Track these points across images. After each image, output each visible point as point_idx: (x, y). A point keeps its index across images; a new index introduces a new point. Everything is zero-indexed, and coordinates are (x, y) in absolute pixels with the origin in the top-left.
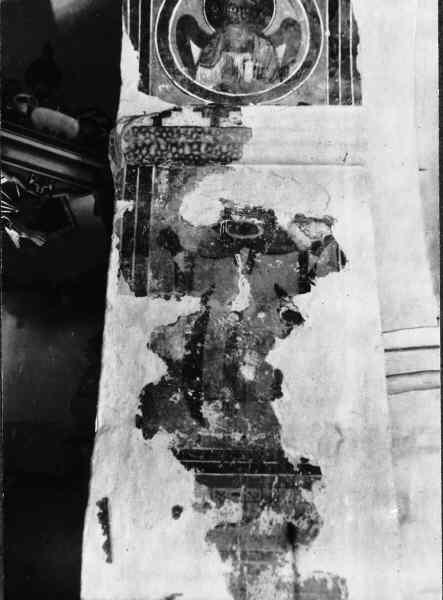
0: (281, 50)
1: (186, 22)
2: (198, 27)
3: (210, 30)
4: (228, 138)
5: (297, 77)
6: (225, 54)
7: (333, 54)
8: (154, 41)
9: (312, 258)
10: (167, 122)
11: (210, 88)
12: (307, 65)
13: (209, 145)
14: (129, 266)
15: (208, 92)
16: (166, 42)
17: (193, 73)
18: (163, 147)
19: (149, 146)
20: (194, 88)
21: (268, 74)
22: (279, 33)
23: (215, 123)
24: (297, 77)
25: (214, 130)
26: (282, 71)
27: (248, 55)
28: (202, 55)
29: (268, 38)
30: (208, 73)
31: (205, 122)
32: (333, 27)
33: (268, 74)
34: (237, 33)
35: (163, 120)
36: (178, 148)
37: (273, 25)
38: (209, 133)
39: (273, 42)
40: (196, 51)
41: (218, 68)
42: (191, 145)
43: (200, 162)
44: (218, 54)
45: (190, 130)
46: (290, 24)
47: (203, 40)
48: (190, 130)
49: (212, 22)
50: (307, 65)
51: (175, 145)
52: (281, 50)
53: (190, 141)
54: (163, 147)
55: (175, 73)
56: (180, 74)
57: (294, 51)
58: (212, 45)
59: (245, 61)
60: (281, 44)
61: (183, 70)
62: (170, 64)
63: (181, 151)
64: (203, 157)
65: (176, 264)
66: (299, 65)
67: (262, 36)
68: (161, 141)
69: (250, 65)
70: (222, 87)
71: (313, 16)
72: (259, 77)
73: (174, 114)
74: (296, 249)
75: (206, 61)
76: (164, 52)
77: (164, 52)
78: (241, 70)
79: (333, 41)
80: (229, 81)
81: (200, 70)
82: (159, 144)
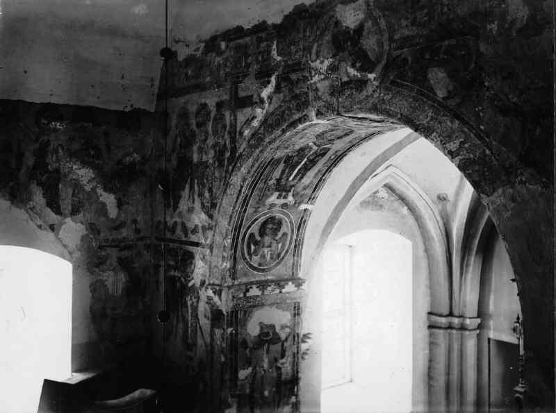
0: (280, 245)
1: (252, 235)
5: (283, 258)
8: (239, 245)
9: (285, 344)
10: (248, 294)
12: (287, 252)
17: (251, 259)
20: (251, 266)
21: (274, 256)
22: (280, 238)
26: (279, 255)
27: (269, 249)
33: (274, 256)
34: (267, 239)
37: (280, 235)
39: (278, 243)
40: (253, 247)
41: (259, 256)
43: (254, 306)
46: (285, 234)
47: (256, 243)
50: (287, 252)
55: (245, 259)
61: (247, 257)
62: (243, 254)
66: (285, 251)
69: (269, 253)
70: (260, 265)
71: (292, 231)
72: (272, 258)
75: (256, 253)
76: (242, 248)
77: (242, 248)
79: (296, 240)
80: (262, 261)
81: (254, 257)
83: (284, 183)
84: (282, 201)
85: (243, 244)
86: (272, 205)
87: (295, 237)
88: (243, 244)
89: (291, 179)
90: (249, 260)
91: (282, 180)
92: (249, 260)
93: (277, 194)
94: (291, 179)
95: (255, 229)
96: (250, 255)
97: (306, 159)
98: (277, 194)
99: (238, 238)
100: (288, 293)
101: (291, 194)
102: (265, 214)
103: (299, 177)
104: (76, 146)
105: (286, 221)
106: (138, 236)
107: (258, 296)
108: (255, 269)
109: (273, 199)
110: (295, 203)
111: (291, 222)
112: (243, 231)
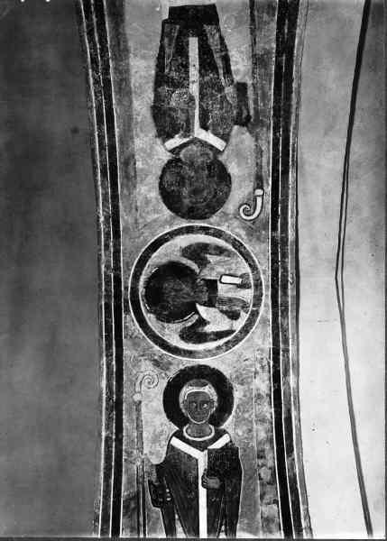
97: (203, 492)
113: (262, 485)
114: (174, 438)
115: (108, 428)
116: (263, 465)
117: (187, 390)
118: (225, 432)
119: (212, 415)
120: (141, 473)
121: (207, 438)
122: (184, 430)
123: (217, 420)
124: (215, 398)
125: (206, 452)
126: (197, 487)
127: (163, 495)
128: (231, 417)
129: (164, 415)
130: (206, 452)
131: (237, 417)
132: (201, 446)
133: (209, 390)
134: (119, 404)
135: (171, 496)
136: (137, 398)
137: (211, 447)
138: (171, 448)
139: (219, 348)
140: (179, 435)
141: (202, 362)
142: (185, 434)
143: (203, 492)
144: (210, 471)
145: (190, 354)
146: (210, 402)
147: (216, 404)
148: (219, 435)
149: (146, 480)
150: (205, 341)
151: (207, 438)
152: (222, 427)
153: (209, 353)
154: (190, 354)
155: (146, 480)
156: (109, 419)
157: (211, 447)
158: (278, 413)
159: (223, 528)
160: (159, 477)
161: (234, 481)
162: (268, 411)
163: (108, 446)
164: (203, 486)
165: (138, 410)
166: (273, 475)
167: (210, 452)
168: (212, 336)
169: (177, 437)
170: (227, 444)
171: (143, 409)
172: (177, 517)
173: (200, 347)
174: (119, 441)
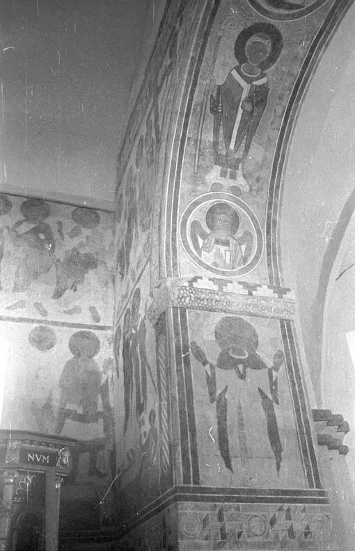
0: (243, 247)
1: (195, 224)
2: (202, 230)
3: (208, 231)
4: (227, 298)
5: (252, 264)
6: (215, 245)
7: (269, 254)
9: (275, 374)
10: (195, 285)
11: (209, 264)
13: (217, 301)
14: (181, 370)
15: (208, 266)
16: (185, 233)
17: (200, 255)
18: (193, 299)
19: (185, 298)
20: (201, 263)
23: (220, 289)
24: (252, 264)
25: (220, 293)
26: (245, 260)
27: (227, 248)
28: (204, 243)
29: (236, 240)
30: (208, 255)
31: (215, 288)
32: (268, 239)
35: (194, 284)
36: (201, 300)
37: (240, 234)
38: (217, 294)
40: (200, 241)
42: (207, 300)
44: (212, 245)
45: (208, 291)
47: (204, 236)
48: (208, 291)
49: (209, 226)
50: (257, 258)
51: (199, 299)
52: (243, 247)
53: (207, 297)
54: (193, 299)
55: (190, 252)
56: (193, 253)
57: (249, 249)
58: (209, 239)
59: (225, 251)
60: (243, 244)
61: (194, 251)
62: (187, 247)
63: (202, 302)
64: (214, 307)
65: (206, 371)
67: (234, 238)
68: (192, 295)
69: (228, 253)
71: (259, 231)
73: (199, 280)
74: (266, 367)
76: (185, 241)
77: (185, 241)
78: (224, 256)
80: (218, 261)
81: (203, 253)
82: (190, 297)
83: (224, 153)
84: (231, 183)
85: (183, 233)
86: (217, 187)
87: (265, 242)
88: (183, 233)
89: (232, 146)
90: (197, 255)
91: (220, 147)
92: (197, 255)
93: (217, 169)
94: (232, 146)
95: (198, 215)
96: (196, 247)
97: (240, 111)
98: (217, 169)
99: (175, 222)
100: (265, 299)
101: (239, 172)
102: (209, 198)
103: (243, 145)
104: (25, 228)
105: (245, 216)
106: (97, 324)
107: (212, 292)
108: (208, 268)
109: (214, 175)
110: (251, 189)
111: (253, 218)
112: (180, 215)
113: (275, 116)
114: (234, 70)
115: (195, 49)
116: (280, 104)
117: (255, 39)
118: (265, 75)
119: (263, 62)
120: (208, 88)
121: (255, 76)
122: (242, 66)
123: (264, 66)
124: (269, 50)
125: (250, 85)
126: (238, 107)
127: (217, 107)
128: (274, 66)
129: (233, 51)
130: (250, 85)
131: (277, 68)
132: (249, 80)
133: (268, 44)
134: (207, 34)
135: (222, 109)
136: (220, 33)
137: (254, 83)
138: (230, 76)
139: (287, 15)
140: (238, 69)
141: (272, 21)
142: (242, 70)
143: (240, 111)
144: (250, 99)
145: (266, 13)
146: (265, 52)
147: (268, 55)
148: (262, 76)
149: (210, 94)
150: (282, 7)
151: (255, 76)
152: (266, 72)
153: (279, 17)
154: (266, 13)
155: (210, 94)
156: (197, 44)
157: (254, 83)
158: (302, 74)
159: (245, 137)
160: (218, 94)
161: (260, 109)
162: (297, 70)
163: (192, 64)
164: (242, 107)
165: (218, 43)
166: (283, 112)
167: (252, 86)
168: (287, 5)
169: (237, 70)
170: (264, 84)
171: (222, 42)
172: (222, 123)
173: (276, 11)
174: (200, 61)
